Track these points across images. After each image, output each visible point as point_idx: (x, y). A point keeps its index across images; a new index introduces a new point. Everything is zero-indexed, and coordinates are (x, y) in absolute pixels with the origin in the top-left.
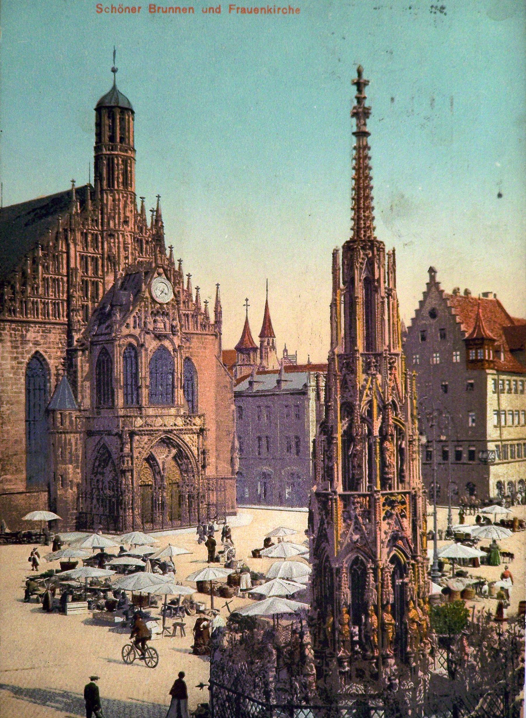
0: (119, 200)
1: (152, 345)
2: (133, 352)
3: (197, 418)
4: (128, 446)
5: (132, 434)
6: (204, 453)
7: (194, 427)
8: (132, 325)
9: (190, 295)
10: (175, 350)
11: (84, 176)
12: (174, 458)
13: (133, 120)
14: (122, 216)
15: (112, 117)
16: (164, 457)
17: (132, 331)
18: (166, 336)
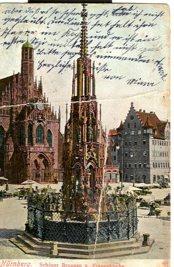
1: (37, 124)
2: (31, 127)
3: (51, 148)
5: (30, 152)
6: (53, 160)
8: (31, 117)
9: (50, 109)
10: (44, 126)
11: (18, 70)
14: (29, 83)
16: (40, 161)
18: (42, 121)
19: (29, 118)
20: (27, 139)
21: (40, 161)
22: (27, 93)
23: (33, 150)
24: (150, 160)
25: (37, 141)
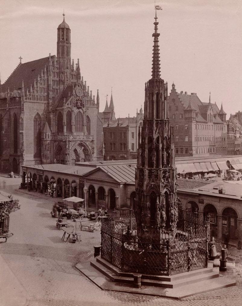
0: (65, 61)
1: (76, 110)
2: (69, 114)
4: (68, 146)
5: (69, 141)
6: (93, 148)
7: (90, 140)
8: (69, 104)
9: (89, 94)
10: (84, 113)
11: (54, 53)
12: (83, 150)
13: (70, 32)
15: (63, 32)
17: (69, 106)
18: (81, 108)
19: (68, 104)
20: (65, 127)
21: (80, 150)
22: (65, 77)
23: (72, 139)
24: (193, 145)
25: (77, 130)
